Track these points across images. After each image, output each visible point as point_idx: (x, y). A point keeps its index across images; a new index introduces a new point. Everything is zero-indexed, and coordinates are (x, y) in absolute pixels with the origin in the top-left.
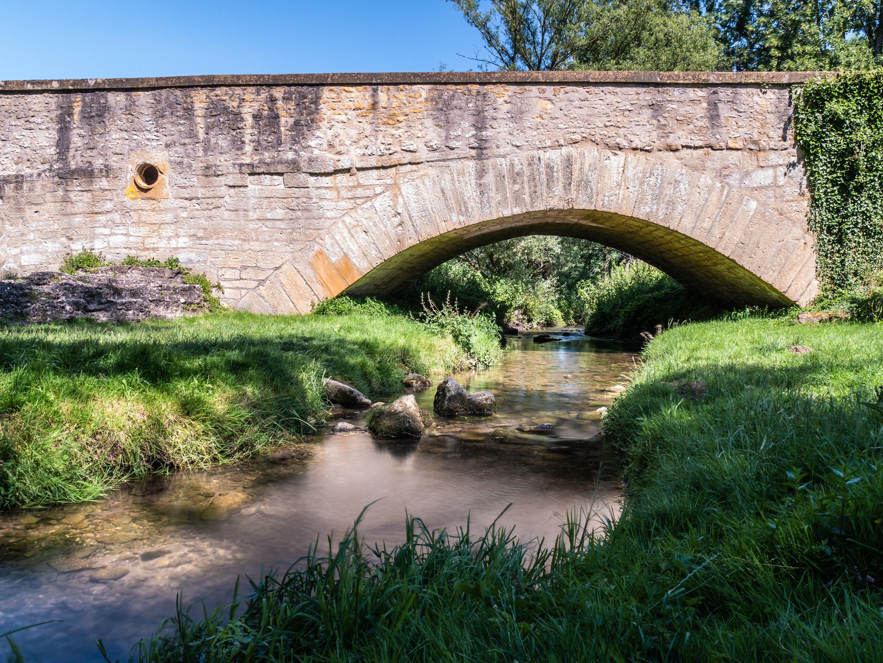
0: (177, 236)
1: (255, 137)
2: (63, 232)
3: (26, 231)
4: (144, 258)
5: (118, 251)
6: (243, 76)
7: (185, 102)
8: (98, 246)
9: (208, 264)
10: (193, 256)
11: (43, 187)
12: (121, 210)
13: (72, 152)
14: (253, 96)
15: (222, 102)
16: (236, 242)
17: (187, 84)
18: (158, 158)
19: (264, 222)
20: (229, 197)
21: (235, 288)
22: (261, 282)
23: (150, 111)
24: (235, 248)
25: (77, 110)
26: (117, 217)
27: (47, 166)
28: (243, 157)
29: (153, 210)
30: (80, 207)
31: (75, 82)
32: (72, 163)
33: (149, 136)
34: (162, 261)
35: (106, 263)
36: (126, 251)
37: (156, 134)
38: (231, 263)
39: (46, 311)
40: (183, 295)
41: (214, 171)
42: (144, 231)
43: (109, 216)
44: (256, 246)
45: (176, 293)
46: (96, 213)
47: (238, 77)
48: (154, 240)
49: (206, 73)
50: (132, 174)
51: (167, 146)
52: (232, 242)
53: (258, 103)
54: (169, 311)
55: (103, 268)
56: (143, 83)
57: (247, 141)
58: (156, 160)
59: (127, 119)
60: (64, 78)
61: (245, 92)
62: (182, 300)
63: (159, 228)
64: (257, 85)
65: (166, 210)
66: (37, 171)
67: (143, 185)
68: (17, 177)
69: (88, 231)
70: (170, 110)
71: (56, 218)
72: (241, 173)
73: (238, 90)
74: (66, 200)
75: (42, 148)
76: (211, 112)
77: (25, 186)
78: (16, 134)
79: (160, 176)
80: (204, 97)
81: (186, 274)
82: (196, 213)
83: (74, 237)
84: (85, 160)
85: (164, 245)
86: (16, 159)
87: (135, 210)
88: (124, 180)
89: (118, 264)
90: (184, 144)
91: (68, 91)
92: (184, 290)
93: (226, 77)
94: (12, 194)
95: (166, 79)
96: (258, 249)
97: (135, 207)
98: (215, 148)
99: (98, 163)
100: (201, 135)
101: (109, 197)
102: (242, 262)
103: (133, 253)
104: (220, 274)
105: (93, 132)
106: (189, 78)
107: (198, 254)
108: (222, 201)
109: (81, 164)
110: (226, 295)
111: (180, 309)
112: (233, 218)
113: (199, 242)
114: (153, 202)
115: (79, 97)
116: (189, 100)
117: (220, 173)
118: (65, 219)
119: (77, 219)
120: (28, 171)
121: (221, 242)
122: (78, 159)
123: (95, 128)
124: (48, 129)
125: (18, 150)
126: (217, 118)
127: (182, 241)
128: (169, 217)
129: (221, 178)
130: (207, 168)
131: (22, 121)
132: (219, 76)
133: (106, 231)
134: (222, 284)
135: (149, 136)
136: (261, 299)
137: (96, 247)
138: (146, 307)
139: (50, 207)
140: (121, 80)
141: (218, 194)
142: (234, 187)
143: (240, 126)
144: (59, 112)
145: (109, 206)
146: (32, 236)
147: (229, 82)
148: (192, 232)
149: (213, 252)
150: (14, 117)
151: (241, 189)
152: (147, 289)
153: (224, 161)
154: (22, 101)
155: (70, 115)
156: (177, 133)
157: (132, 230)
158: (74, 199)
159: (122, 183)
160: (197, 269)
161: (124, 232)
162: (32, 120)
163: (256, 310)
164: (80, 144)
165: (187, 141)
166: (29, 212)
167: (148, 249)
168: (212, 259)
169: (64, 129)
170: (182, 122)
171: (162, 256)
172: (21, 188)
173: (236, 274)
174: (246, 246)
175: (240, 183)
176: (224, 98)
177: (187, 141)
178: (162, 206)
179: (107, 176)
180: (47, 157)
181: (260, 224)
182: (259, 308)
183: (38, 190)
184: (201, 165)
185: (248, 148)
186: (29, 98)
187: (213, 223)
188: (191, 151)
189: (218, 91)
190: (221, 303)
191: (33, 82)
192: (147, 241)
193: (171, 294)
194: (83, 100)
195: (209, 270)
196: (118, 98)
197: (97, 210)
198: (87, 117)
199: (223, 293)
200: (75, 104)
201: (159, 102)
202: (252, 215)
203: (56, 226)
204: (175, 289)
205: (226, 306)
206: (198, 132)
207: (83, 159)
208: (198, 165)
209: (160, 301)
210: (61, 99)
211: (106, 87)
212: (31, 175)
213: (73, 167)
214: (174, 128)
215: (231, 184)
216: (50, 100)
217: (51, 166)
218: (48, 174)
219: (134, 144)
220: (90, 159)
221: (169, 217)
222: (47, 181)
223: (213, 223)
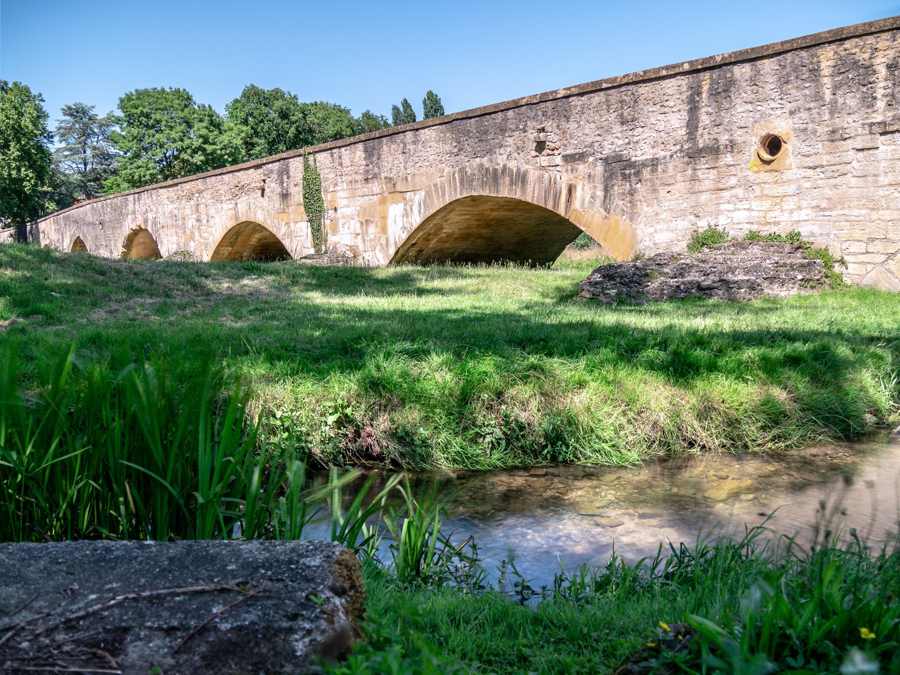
0: (800, 208)
1: (888, 90)
2: (691, 210)
3: (659, 211)
4: (765, 233)
5: (740, 226)
6: (877, 21)
7: (811, 63)
8: (722, 222)
9: (832, 236)
10: (816, 230)
11: (674, 169)
12: (745, 185)
13: (700, 131)
14: (887, 43)
15: (852, 57)
16: (864, 212)
17: (813, 43)
18: (781, 127)
19: (896, 187)
20: (858, 162)
21: (860, 263)
22: (891, 256)
23: (775, 78)
24: (863, 218)
25: (705, 88)
26: (740, 192)
27: (678, 147)
28: (874, 115)
29: (776, 182)
30: (707, 184)
31: (704, 61)
32: (701, 141)
33: (773, 105)
34: (783, 235)
35: (729, 239)
36: (749, 226)
37: (780, 101)
38: (857, 234)
39: (663, 290)
40: (801, 272)
41: (841, 135)
42: (767, 204)
43: (733, 192)
44: (886, 214)
45: (793, 269)
46: (721, 190)
47: (871, 24)
48: (776, 213)
49: (834, 27)
50: (756, 147)
51: (792, 113)
52: (859, 211)
53: (893, 50)
54: (785, 288)
55: (726, 244)
56: (768, 49)
57: (879, 96)
58: (780, 130)
59: (752, 91)
60: (694, 59)
61: (879, 39)
62: (800, 277)
63: (782, 201)
64: (893, 29)
65: (789, 181)
66: (669, 153)
67: (767, 156)
68: (653, 160)
69: (713, 208)
70: (795, 74)
71: (685, 196)
72: (871, 133)
73: (870, 40)
74: (694, 179)
75: (674, 130)
76: (839, 69)
77: (660, 168)
78: (653, 120)
79: (784, 145)
80: (832, 53)
81: (807, 248)
82: (820, 182)
83: (701, 214)
84: (712, 137)
85: (785, 219)
86: (652, 143)
87: (758, 184)
88: (747, 154)
89: (740, 240)
90: (809, 109)
91: (698, 71)
92: (802, 266)
93: (856, 27)
94: (649, 177)
95: (792, 41)
96: (889, 218)
97: (758, 181)
98: (842, 109)
99: (724, 139)
100: (828, 96)
101: (733, 172)
102: (870, 233)
103: (755, 228)
104: (844, 248)
105: (719, 109)
106: (815, 35)
107: (821, 227)
108: (849, 166)
109: (708, 142)
110: (850, 270)
111: (797, 286)
112: (861, 184)
113: (822, 213)
114: (777, 174)
115: (707, 75)
116: (815, 60)
117: (848, 136)
118: (693, 197)
119: (704, 197)
120: (662, 154)
121: (846, 212)
122: (706, 137)
123: (722, 104)
124: (679, 111)
125: (654, 135)
126: (845, 75)
127: (803, 215)
128: (791, 189)
129: (848, 141)
130: (833, 132)
131: (658, 106)
132: (848, 27)
133: (730, 207)
134: (846, 258)
135: (773, 105)
136: (889, 275)
137: (720, 223)
138: (759, 285)
139: (681, 187)
140: (747, 51)
141: (845, 160)
142: (863, 150)
143: (871, 80)
144: (689, 93)
145: (733, 181)
146: (664, 216)
147: (860, 32)
148: (815, 203)
149: (837, 224)
150: (651, 104)
151: (871, 152)
152: (761, 266)
153: (851, 123)
154: (658, 87)
155: (699, 94)
156: (802, 98)
157: (755, 205)
158: (701, 177)
159: (745, 157)
160: (820, 243)
161: (747, 207)
162: (666, 104)
163: (884, 286)
164: (707, 122)
165: (812, 105)
166: (662, 193)
167: (769, 223)
168: (836, 232)
169: (693, 109)
170: (807, 85)
171: (783, 230)
172: (657, 170)
173: (862, 247)
174: (875, 216)
175: (870, 145)
176: (853, 51)
177: (812, 105)
178: (785, 177)
179: (732, 152)
180: (678, 138)
181: (892, 189)
182: (887, 285)
183: (671, 171)
184: (826, 129)
185: (881, 104)
186: (664, 83)
187: (839, 191)
188: (816, 115)
189: (848, 44)
190: (844, 279)
191: (667, 68)
192: (770, 215)
193: (788, 270)
194: (711, 78)
195: (831, 243)
196: (743, 70)
197: (721, 186)
198: (714, 94)
199: (847, 268)
200: (704, 83)
201: (784, 67)
202: (883, 180)
203: (685, 205)
204: (792, 266)
205: (849, 282)
206: (824, 93)
207: (711, 136)
208: (823, 130)
209: (775, 278)
210: (691, 79)
211: (733, 60)
212: (665, 158)
213: (701, 146)
214: (798, 93)
215: (860, 147)
216: (682, 82)
217: (682, 146)
218: (679, 155)
219: (758, 115)
220: (716, 136)
221: (791, 189)
222: (679, 161)
223: (839, 191)
